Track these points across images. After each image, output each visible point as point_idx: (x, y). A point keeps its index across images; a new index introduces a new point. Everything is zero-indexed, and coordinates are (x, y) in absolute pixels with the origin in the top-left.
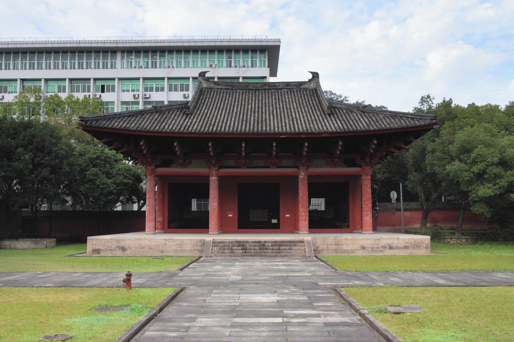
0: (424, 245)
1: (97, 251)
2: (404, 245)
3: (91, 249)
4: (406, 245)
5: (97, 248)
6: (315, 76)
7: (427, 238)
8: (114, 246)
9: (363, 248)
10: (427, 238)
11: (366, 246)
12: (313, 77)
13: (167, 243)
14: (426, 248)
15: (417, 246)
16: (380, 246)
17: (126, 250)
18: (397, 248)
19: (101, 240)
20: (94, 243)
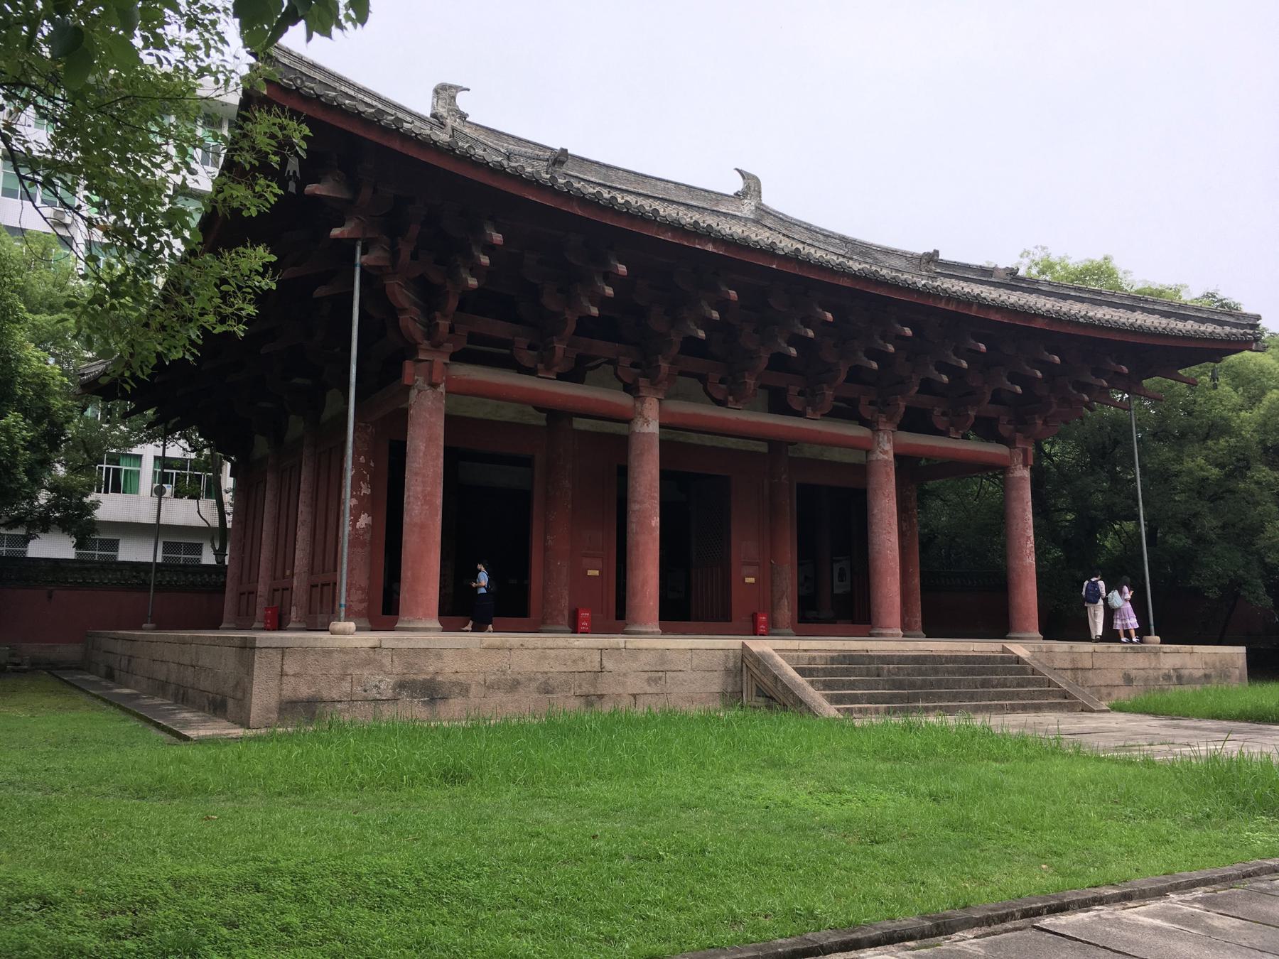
0: (1237, 672)
1: (303, 709)
2: (1201, 673)
3: (273, 702)
4: (1207, 672)
5: (305, 691)
6: (752, 186)
7: (1236, 654)
8: (386, 685)
9: (1128, 680)
10: (1236, 654)
11: (1133, 673)
12: (748, 187)
13: (609, 665)
14: (1241, 679)
15: (1224, 675)
16: (1161, 672)
17: (445, 698)
18: (1192, 680)
19: (328, 653)
20: (289, 669)
